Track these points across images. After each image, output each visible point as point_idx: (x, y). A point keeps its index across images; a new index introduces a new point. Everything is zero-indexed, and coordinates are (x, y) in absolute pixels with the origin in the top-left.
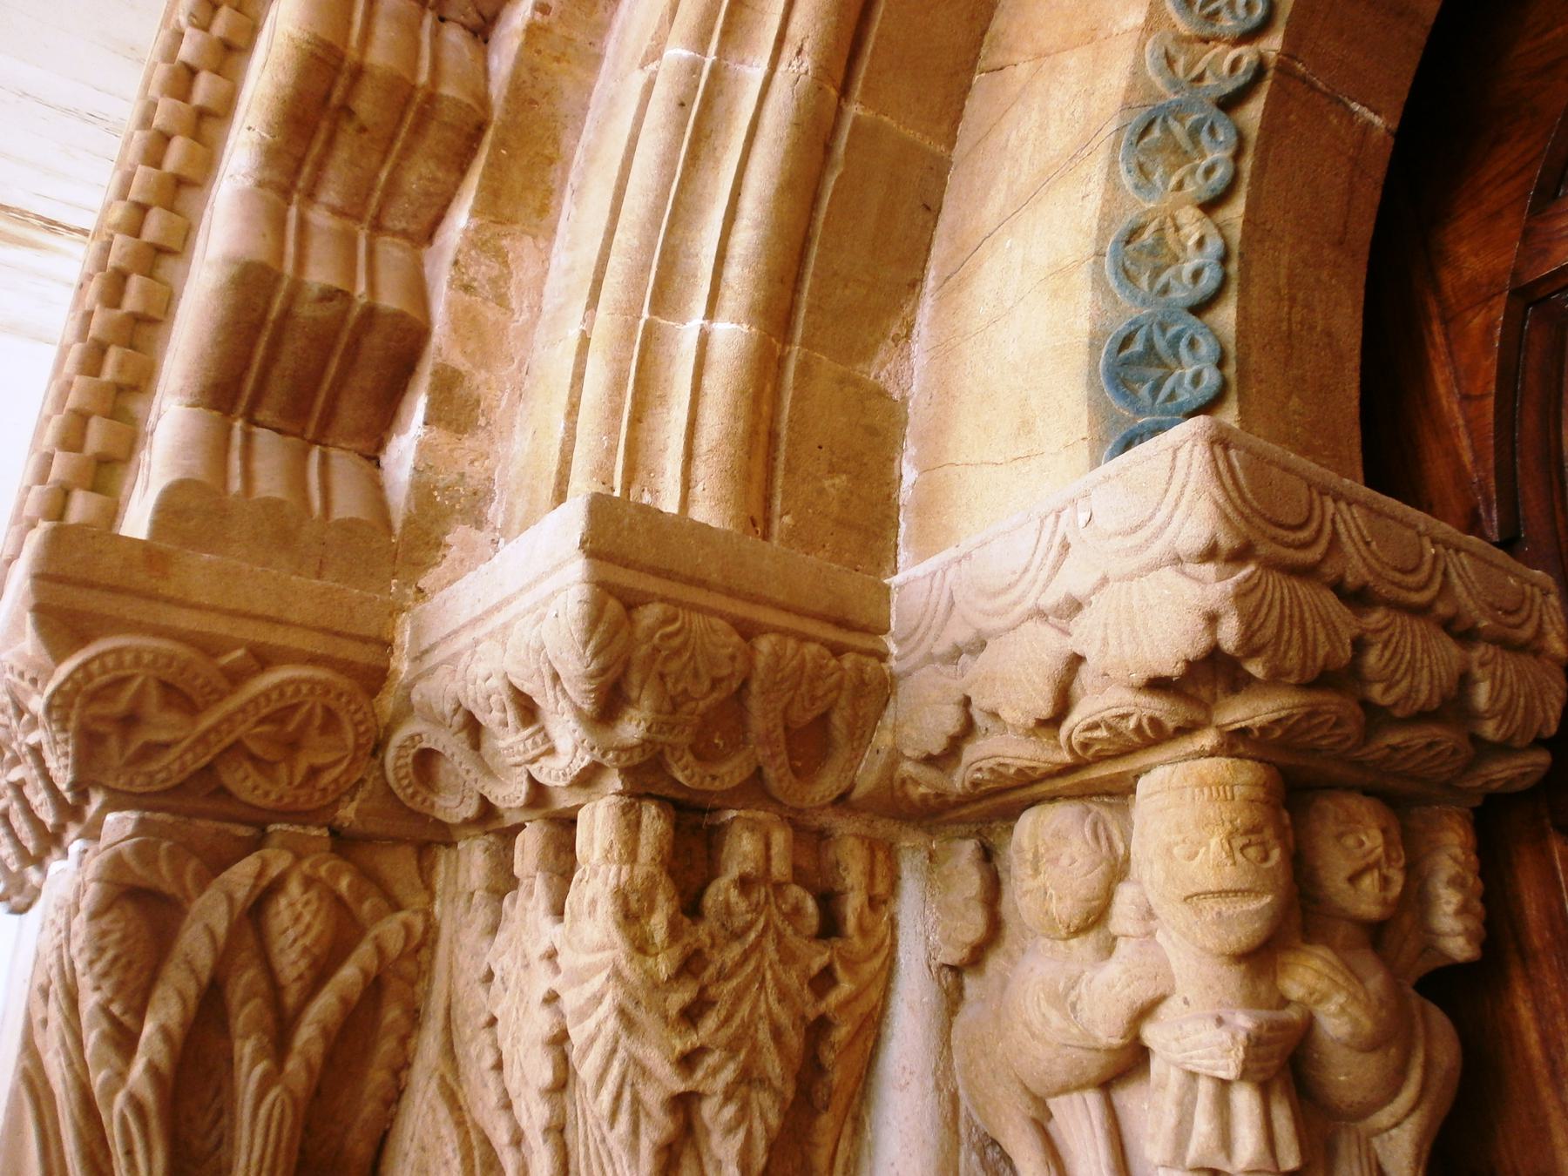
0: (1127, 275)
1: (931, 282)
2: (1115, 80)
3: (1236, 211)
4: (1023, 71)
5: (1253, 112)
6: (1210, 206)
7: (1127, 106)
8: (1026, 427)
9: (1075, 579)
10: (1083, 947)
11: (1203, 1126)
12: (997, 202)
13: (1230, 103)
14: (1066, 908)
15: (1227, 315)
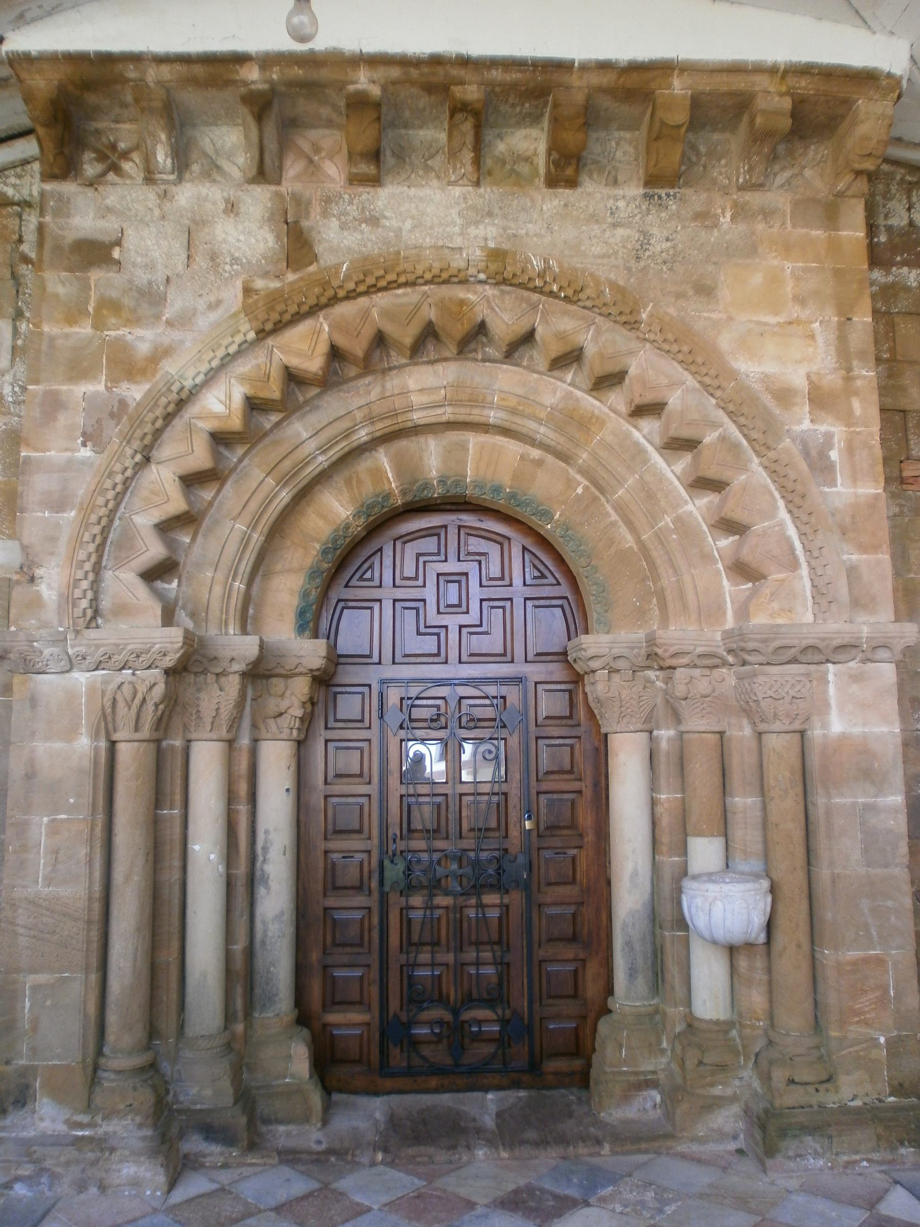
0: (304, 597)
1: (260, 573)
2: (309, 561)
3: (319, 590)
4: (289, 543)
5: (325, 574)
6: (316, 588)
7: (310, 568)
8: (281, 615)
9: (302, 653)
10: (280, 699)
11: (293, 722)
12: (279, 567)
13: (323, 572)
14: (280, 693)
15: (314, 607)
